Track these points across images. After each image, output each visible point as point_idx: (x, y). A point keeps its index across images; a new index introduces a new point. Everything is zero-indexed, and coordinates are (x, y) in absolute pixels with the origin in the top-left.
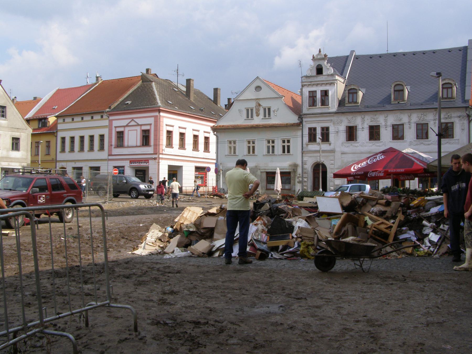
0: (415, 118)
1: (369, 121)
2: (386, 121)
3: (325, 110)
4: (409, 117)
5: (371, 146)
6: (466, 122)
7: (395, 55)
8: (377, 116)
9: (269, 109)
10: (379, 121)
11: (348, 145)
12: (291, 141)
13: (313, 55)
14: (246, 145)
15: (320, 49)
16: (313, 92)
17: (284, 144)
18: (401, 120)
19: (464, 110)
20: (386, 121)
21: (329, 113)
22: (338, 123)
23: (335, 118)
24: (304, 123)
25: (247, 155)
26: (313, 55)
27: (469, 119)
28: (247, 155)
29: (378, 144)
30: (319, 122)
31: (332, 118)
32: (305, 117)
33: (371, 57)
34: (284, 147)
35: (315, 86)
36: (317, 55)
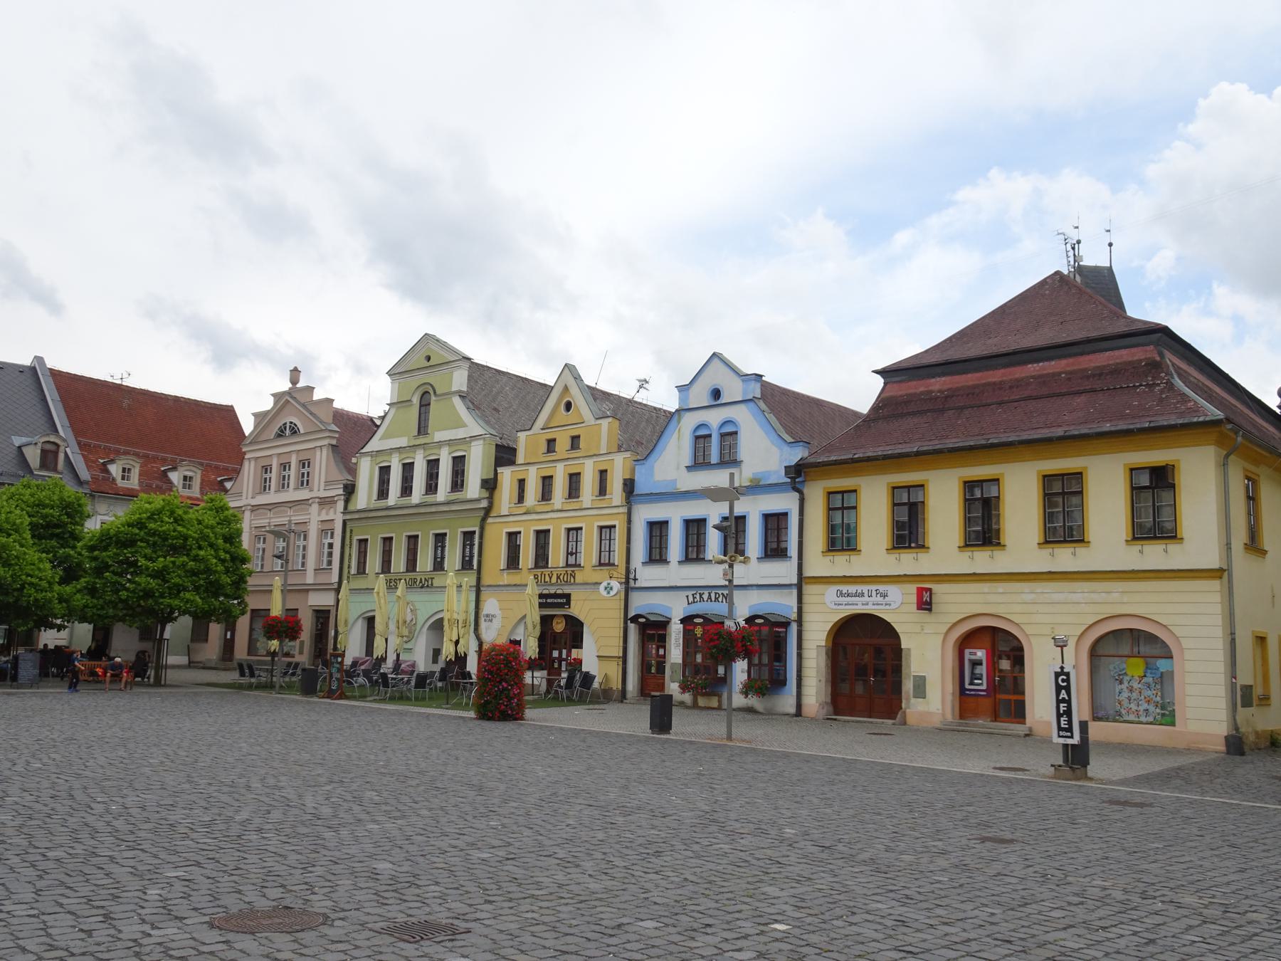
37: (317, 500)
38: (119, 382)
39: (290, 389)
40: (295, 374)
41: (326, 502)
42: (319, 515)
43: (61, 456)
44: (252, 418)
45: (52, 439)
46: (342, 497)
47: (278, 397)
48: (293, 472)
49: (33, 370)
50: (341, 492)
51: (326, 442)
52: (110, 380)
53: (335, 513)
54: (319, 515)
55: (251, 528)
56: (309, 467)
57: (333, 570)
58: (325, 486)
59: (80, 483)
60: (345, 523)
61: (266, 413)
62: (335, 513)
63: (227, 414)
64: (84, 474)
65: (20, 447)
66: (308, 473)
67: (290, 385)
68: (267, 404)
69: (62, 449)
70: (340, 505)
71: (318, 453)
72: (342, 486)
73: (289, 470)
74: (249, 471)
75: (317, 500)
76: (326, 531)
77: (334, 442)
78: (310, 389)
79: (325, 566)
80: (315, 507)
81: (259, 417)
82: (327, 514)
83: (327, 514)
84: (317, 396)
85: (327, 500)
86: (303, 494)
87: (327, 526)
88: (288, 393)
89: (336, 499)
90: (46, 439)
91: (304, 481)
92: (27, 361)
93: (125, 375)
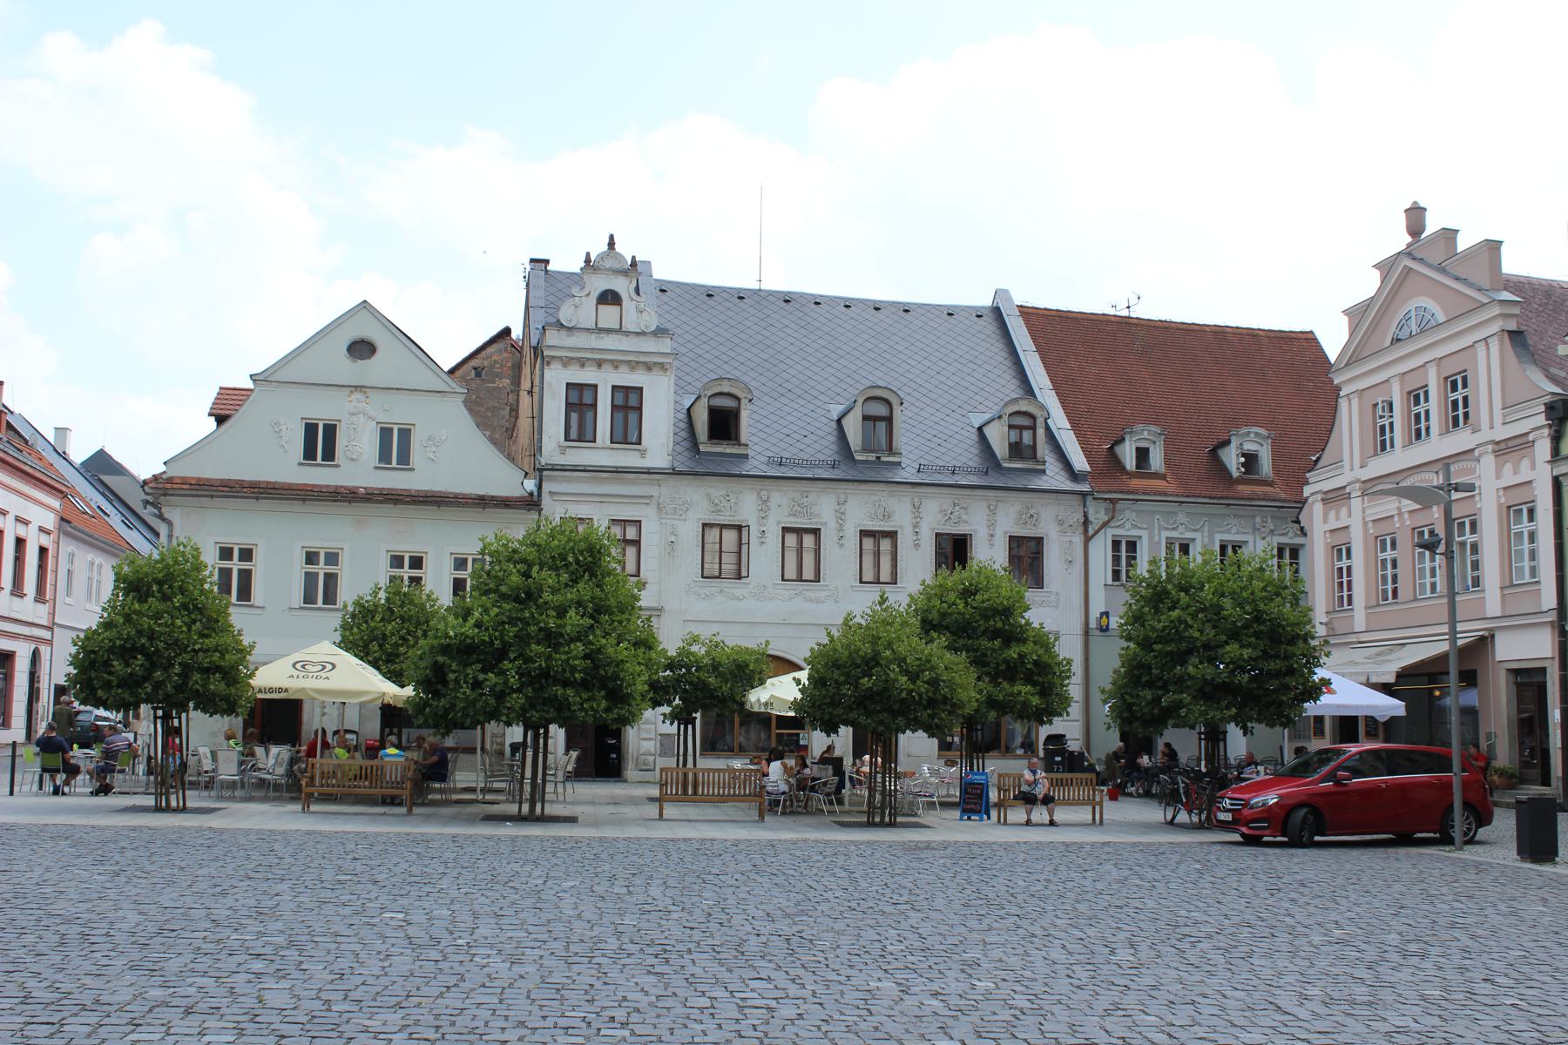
0: (782, 507)
1: (786, 512)
2: (840, 516)
3: (625, 458)
4: (916, 508)
5: (791, 599)
6: (1078, 540)
7: (787, 299)
8: (812, 497)
9: (405, 434)
10: (818, 516)
11: (707, 591)
12: (344, 559)
13: (588, 254)
14: (297, 569)
15: (612, 237)
16: (580, 387)
17: (226, 564)
18: (887, 516)
19: (1075, 501)
20: (840, 516)
21: (649, 472)
22: (675, 511)
23: (666, 490)
24: (546, 501)
25: (301, 608)
26: (588, 254)
27: (1086, 531)
28: (301, 608)
29: (812, 595)
30: (602, 498)
31: (652, 490)
32: (551, 479)
33: (710, 293)
34: (310, 579)
35: (624, 368)
36: (601, 257)
37: (1490, 448)
38: (1125, 313)
39: (1409, 245)
40: (1415, 216)
41: (1508, 449)
42: (1498, 476)
43: (1041, 432)
44: (1345, 319)
45: (1024, 406)
46: (1546, 431)
47: (1385, 267)
48: (1434, 405)
49: (997, 312)
50: (1541, 420)
51: (1495, 328)
52: (1112, 312)
53: (1533, 467)
54: (1498, 476)
55: (1365, 523)
56: (1465, 386)
57: (1542, 586)
58: (1504, 416)
59: (1074, 475)
60: (1557, 484)
61: (1366, 306)
62: (1533, 467)
63: (1306, 342)
64: (1080, 462)
65: (980, 429)
66: (1465, 399)
67: (1409, 239)
68: (1368, 285)
69: (1040, 422)
70: (1543, 448)
71: (1481, 350)
72: (1542, 408)
73: (1427, 400)
74: (1350, 422)
75: (1490, 448)
76: (1518, 509)
77: (1512, 326)
78: (1449, 235)
79: (1527, 579)
80: (1488, 462)
81: (1356, 315)
82: (1516, 472)
83: (1516, 472)
84: (1463, 244)
85: (1511, 444)
86: (1461, 440)
87: (1518, 497)
88: (1408, 253)
89: (1531, 437)
90: (1016, 408)
91: (1459, 415)
92: (986, 301)
93: (1133, 301)
